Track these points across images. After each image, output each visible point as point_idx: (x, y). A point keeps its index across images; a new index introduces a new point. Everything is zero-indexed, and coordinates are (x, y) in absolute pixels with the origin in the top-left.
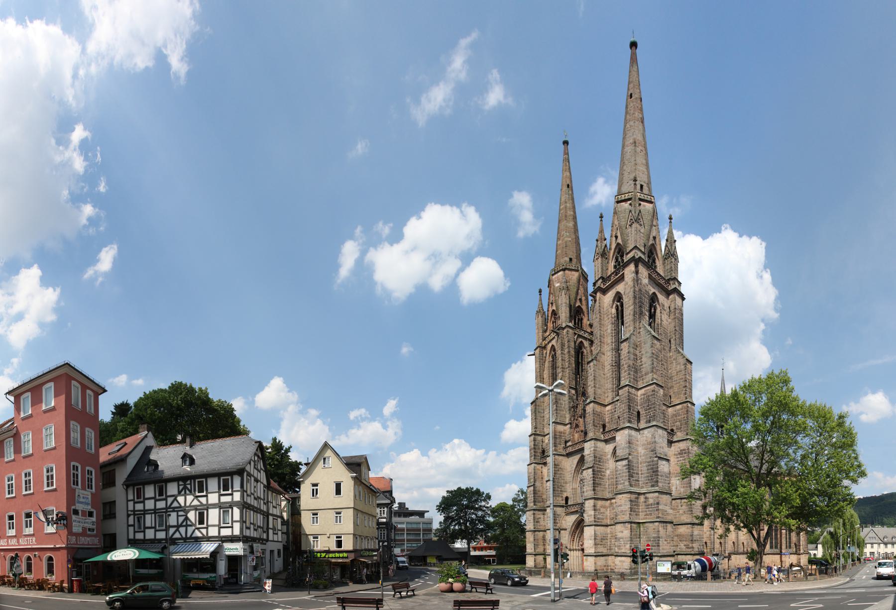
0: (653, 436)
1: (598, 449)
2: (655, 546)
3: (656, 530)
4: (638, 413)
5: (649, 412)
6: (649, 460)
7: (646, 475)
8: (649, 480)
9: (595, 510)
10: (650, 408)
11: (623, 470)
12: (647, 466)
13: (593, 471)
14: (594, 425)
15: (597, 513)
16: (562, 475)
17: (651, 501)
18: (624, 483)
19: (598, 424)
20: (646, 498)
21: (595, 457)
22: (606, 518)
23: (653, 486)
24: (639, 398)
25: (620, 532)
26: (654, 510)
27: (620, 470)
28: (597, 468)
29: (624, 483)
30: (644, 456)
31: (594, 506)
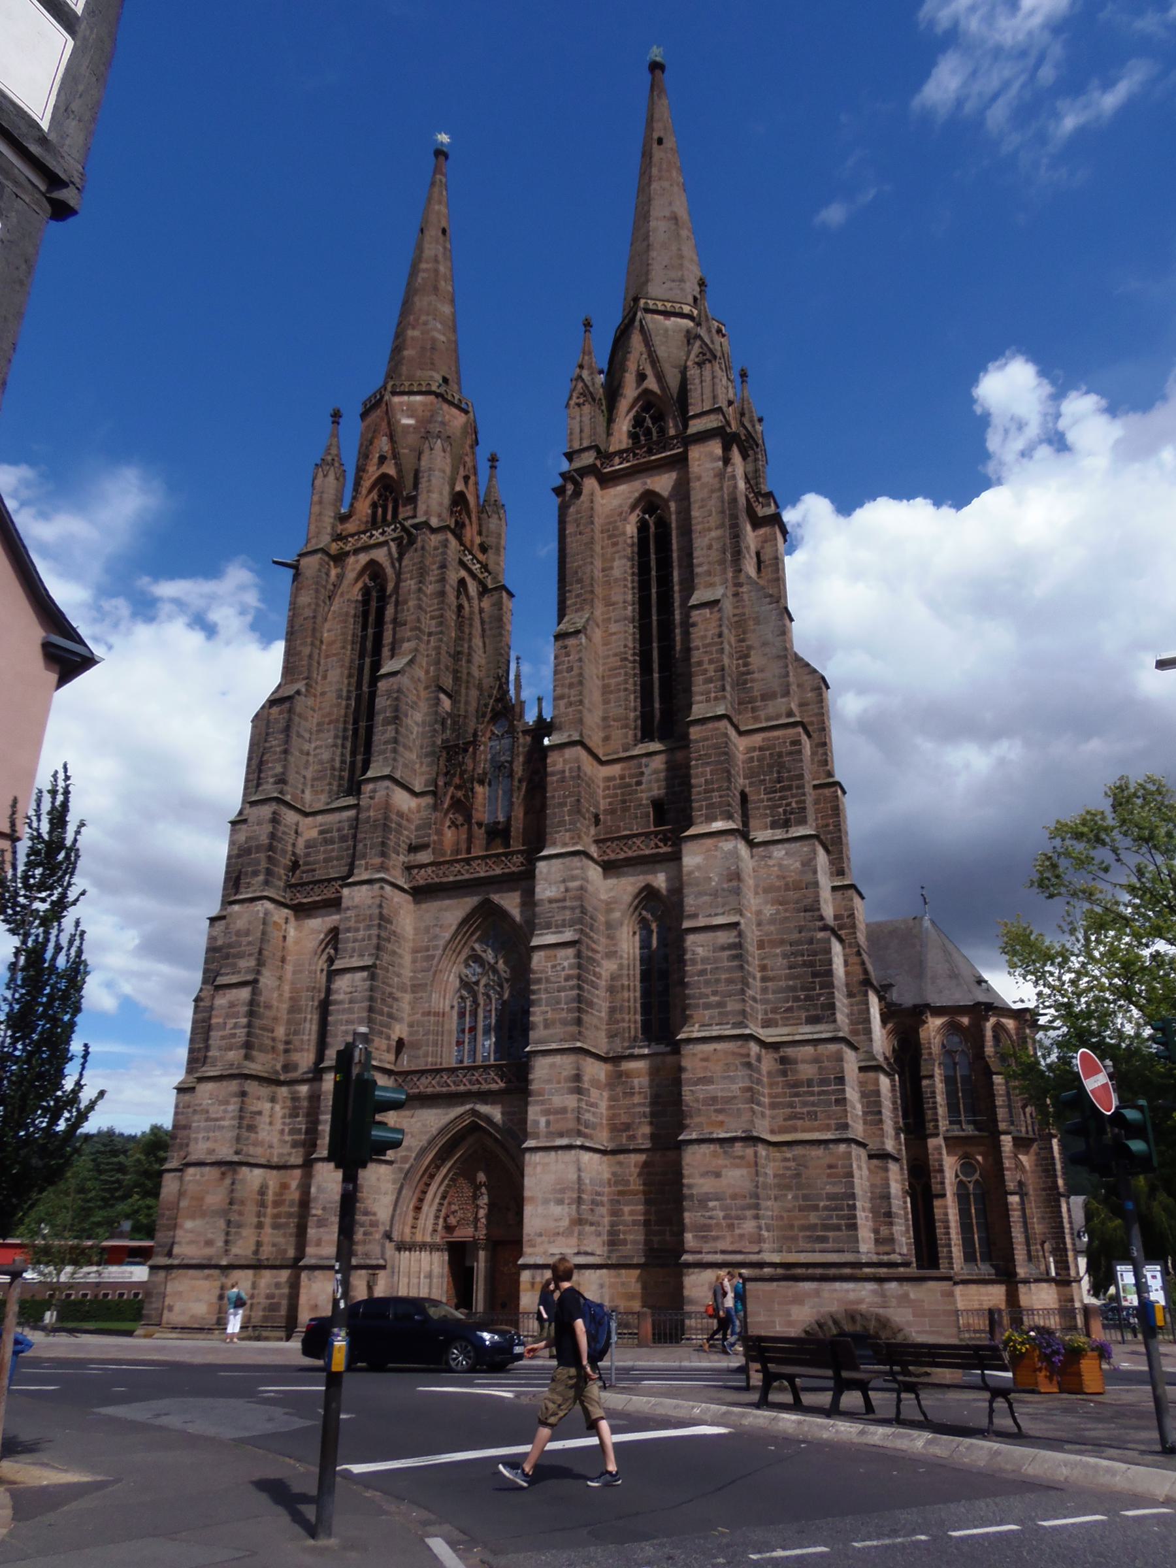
2: (838, 1228)
3: (840, 1170)
4: (744, 797)
5: (781, 798)
6: (795, 936)
7: (783, 984)
8: (796, 999)
9: (579, 1091)
11: (716, 960)
12: (785, 956)
13: (579, 955)
17: (807, 1071)
20: (784, 1060)
23: (813, 1020)
25: (705, 1174)
26: (828, 1103)
27: (705, 960)
29: (720, 1005)
30: (772, 921)
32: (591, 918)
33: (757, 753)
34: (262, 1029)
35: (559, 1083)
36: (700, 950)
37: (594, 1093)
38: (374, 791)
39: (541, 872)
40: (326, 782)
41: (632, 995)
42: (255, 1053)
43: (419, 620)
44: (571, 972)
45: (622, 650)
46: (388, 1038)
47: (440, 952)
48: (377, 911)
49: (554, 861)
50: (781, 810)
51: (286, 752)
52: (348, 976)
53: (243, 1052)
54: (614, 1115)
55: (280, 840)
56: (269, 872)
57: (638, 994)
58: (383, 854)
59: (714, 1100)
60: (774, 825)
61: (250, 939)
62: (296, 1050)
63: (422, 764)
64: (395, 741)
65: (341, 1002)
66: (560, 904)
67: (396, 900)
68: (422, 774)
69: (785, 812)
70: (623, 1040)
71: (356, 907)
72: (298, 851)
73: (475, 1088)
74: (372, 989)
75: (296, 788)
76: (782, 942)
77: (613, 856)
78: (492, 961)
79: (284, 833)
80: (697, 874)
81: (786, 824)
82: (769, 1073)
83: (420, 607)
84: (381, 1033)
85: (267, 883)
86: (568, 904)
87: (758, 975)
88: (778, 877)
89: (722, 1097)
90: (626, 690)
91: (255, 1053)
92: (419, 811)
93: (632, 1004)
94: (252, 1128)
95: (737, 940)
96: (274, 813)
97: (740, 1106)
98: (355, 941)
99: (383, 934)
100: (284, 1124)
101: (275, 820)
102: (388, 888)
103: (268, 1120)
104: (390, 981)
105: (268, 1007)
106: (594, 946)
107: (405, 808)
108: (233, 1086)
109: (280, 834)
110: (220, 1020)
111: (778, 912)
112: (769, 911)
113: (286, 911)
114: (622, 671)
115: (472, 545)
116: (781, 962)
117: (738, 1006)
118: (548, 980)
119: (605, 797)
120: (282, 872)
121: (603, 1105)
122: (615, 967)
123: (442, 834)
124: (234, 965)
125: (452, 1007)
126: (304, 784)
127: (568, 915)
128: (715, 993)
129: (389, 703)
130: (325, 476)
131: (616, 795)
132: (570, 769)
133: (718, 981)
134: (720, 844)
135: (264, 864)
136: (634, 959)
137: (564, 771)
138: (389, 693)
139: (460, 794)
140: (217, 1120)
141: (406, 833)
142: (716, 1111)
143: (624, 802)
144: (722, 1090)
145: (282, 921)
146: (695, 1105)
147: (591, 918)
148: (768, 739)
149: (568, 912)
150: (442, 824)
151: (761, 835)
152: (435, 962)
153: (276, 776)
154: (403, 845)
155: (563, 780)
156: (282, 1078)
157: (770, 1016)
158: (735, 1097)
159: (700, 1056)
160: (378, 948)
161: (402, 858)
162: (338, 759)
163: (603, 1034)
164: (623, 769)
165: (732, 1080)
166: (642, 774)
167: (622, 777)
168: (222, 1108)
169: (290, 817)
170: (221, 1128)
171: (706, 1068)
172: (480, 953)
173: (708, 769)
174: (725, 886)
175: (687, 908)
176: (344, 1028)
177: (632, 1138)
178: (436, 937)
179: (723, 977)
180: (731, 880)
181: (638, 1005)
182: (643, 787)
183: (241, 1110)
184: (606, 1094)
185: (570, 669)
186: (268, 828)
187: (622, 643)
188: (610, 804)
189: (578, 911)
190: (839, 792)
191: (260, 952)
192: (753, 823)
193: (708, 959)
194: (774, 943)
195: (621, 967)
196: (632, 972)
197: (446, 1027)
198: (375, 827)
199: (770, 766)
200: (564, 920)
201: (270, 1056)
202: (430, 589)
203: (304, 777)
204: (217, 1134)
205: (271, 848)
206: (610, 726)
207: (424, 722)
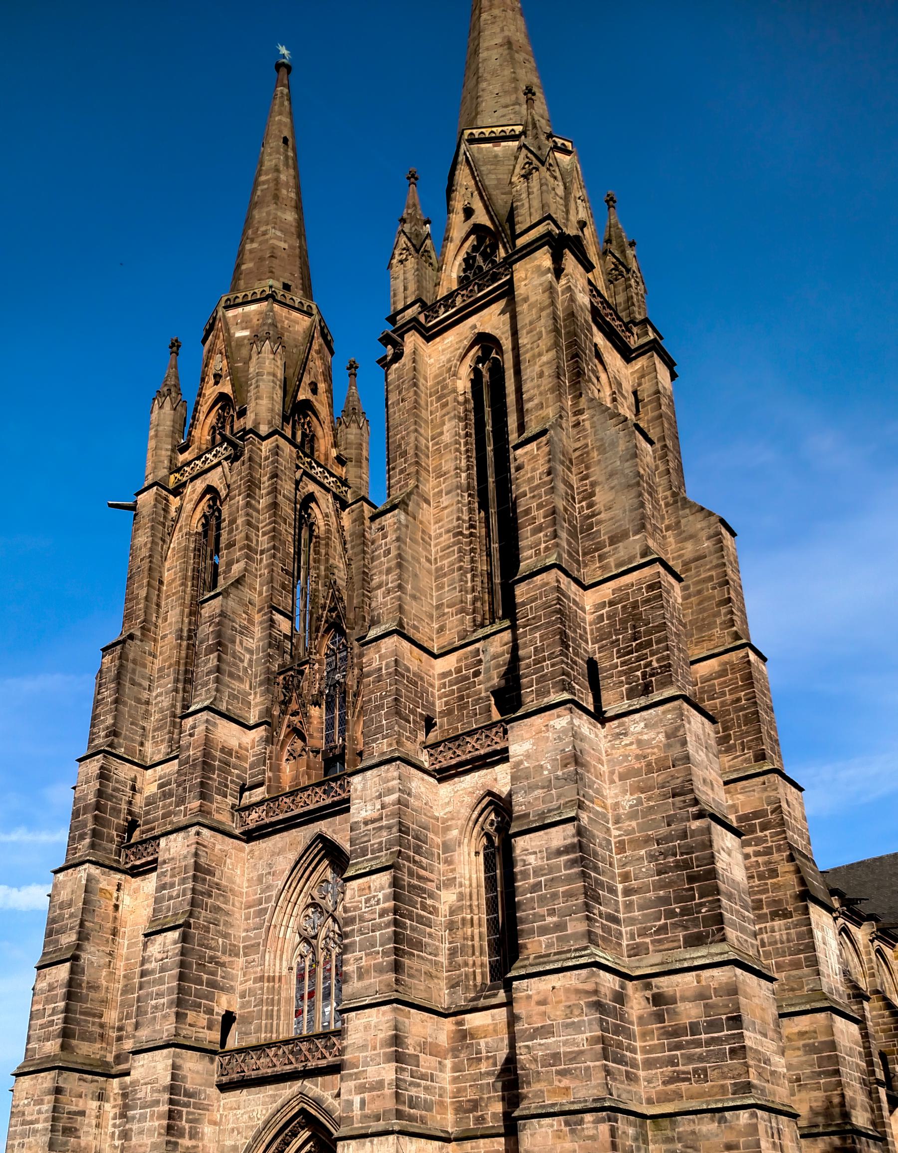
0: (676, 736)
1: (412, 800)
4: (592, 664)
5: (639, 659)
6: (664, 830)
7: (651, 895)
9: (398, 1058)
10: (649, 644)
11: (551, 870)
12: (652, 857)
14: (398, 713)
15: (406, 1076)
16: (223, 919)
18: (560, 927)
19: (412, 712)
21: (403, 829)
22: (441, 1104)
24: (589, 618)
27: (537, 872)
28: (411, 874)
29: (560, 927)
30: (633, 816)
31: (397, 1040)
32: (417, 838)
33: (607, 609)
34: (82, 1013)
35: (375, 1048)
36: (531, 859)
37: (427, 1063)
38: (194, 727)
39: (356, 790)
40: (166, 731)
41: (476, 931)
42: (74, 1042)
43: (248, 538)
44: (387, 905)
45: (455, 523)
46: (210, 1011)
47: (273, 903)
48: (193, 861)
49: (369, 773)
50: (639, 673)
51: (116, 701)
52: (160, 938)
53: (59, 1041)
54: (459, 1090)
55: (110, 798)
56: (95, 834)
57: (484, 929)
58: (203, 796)
59: (556, 1056)
60: (631, 694)
61: (73, 910)
62: (128, 1037)
63: (255, 693)
64: (218, 669)
65: (152, 972)
66: (376, 825)
67: (218, 847)
68: (256, 705)
69: (644, 675)
70: (467, 988)
71: (173, 859)
72: (136, 810)
73: (300, 1067)
74: (183, 953)
75: (133, 741)
76: (647, 841)
77: (445, 764)
78: (331, 909)
79: (115, 789)
80: (526, 764)
81: (647, 690)
82: (640, 1018)
83: (249, 523)
84: (199, 1005)
85: (93, 846)
86: (384, 823)
87: (620, 887)
88: (637, 757)
89: (566, 1054)
90: (460, 568)
91: (74, 1042)
92: (253, 747)
93: (477, 943)
94: (69, 1131)
95: (576, 840)
96: (102, 768)
97: (589, 1063)
98: (170, 899)
99: (199, 887)
100: (114, 1126)
101: (104, 775)
102: (205, 832)
103: (94, 1122)
104: (213, 944)
105: (94, 987)
106: (422, 872)
107: (233, 743)
108: (46, 1080)
109: (110, 791)
110: (41, 1007)
111: (640, 802)
112: (627, 801)
113: (118, 876)
114: (456, 548)
115: (327, 459)
116: (648, 866)
117: (582, 927)
118: (362, 919)
119: (440, 698)
120: (115, 833)
121: (446, 1078)
122: (454, 897)
123: (279, 770)
124: (57, 941)
125: (291, 969)
126: (144, 736)
127: (384, 836)
128: (552, 912)
129: (211, 629)
130: (161, 407)
131: (453, 692)
132: (387, 665)
133: (555, 896)
134: (552, 723)
135: (90, 826)
136: (478, 886)
137: (381, 669)
138: (212, 617)
139: (296, 719)
140: (31, 1122)
141: (236, 772)
142: (558, 1073)
143: (461, 698)
144: (565, 1043)
145: (113, 889)
146: (533, 1067)
147: (417, 838)
148: (620, 589)
149: (384, 833)
150: (279, 759)
151: (611, 708)
152: (267, 916)
153: (107, 728)
154: (233, 786)
155: (379, 679)
156: (114, 1071)
157: (638, 940)
158: (581, 1052)
159: (535, 998)
160: (193, 903)
161: (230, 800)
162: (179, 705)
163: (443, 984)
164: (459, 661)
165: (576, 1027)
166: (480, 661)
167: (459, 670)
168: (37, 1108)
169: (124, 772)
170: (35, 1132)
171: (544, 1013)
172: (318, 900)
173: (537, 635)
174: (560, 773)
175: (516, 808)
176: (153, 1002)
177: (481, 1119)
178: (269, 888)
179: (561, 889)
180: (566, 766)
181: (485, 944)
182: (481, 677)
183: (55, 1109)
184: (448, 1063)
185: (388, 552)
186: (95, 785)
187: (455, 517)
188: (446, 703)
189: (395, 830)
190: (752, 657)
191: (82, 925)
192: (605, 696)
193: (542, 868)
194: (637, 844)
195: (461, 897)
196: (475, 903)
197: (284, 994)
198: (194, 766)
199: (623, 622)
200: (381, 843)
201: (98, 1045)
202: (263, 503)
203: (144, 728)
204: (31, 1139)
205: (98, 807)
206: (444, 614)
207: (258, 648)
